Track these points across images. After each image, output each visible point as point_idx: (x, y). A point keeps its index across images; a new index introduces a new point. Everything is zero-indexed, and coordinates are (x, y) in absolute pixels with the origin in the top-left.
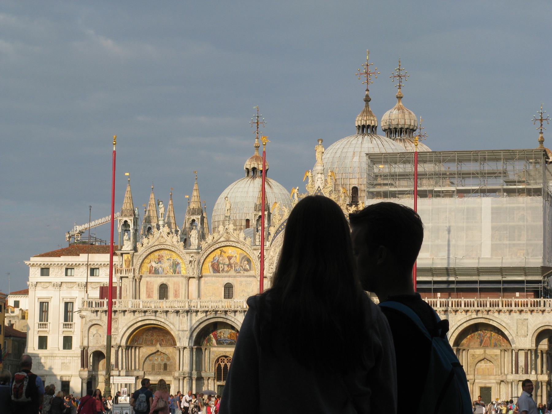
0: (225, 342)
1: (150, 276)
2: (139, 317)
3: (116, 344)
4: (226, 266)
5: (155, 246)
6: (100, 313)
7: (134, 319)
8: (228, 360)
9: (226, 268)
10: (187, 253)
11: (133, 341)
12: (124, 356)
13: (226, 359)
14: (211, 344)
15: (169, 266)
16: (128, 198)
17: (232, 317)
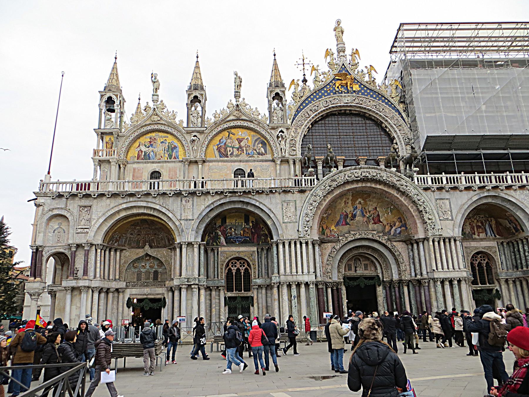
0: (238, 240)
1: (138, 162)
2: (122, 204)
3: (87, 241)
4: (236, 149)
5: (146, 125)
6: (65, 200)
7: (115, 206)
8: (240, 263)
9: (236, 152)
10: (187, 133)
11: (111, 239)
12: (98, 259)
13: (238, 263)
14: (219, 244)
15: (163, 150)
16: (115, 74)
17: (256, 200)
